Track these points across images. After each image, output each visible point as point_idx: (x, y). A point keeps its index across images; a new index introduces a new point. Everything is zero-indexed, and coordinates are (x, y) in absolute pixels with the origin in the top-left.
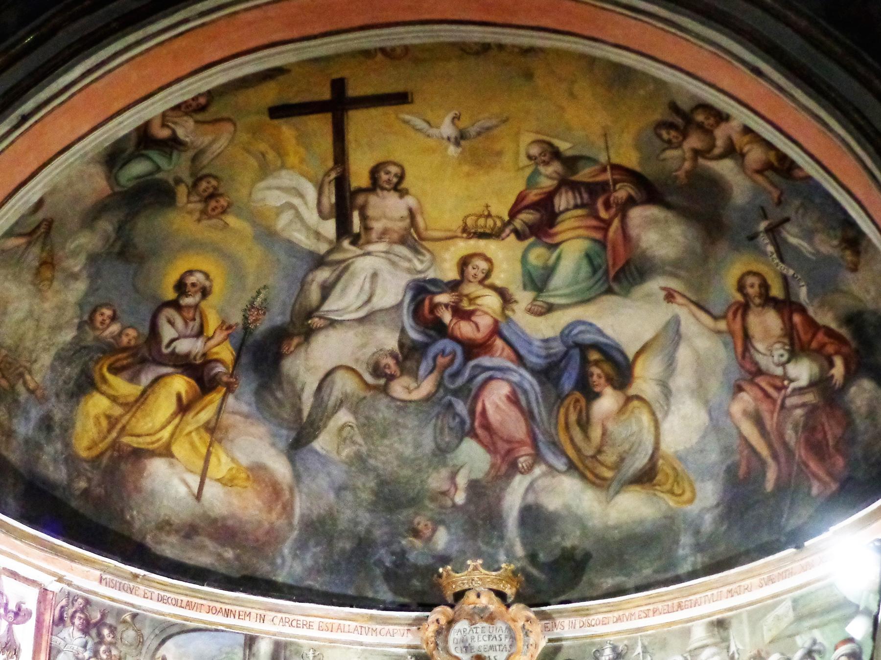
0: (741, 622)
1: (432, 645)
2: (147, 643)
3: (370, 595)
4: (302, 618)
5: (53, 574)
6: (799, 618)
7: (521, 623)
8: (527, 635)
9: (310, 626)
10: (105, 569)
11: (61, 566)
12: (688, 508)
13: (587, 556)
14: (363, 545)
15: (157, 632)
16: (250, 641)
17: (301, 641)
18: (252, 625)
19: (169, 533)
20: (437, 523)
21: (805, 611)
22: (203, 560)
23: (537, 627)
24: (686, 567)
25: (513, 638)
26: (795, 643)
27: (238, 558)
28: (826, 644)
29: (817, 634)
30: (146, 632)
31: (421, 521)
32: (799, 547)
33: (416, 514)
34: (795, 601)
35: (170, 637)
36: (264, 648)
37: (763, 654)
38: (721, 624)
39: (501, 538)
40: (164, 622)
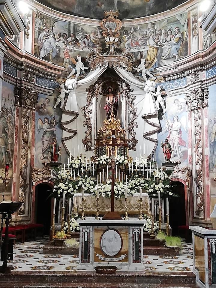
0: (157, 24)
1: (102, 26)
2: (52, 23)
3: (90, 16)
4: (79, 20)
5: (35, 8)
6: (168, 23)
7: (118, 23)
8: (119, 25)
9: (80, 21)
10: (44, 7)
11: (37, 6)
12: (148, 3)
13: (130, 11)
14: (89, 7)
15: (53, 21)
16: (70, 23)
17: (78, 24)
18: (70, 20)
19: (54, 2)
20: (102, 3)
21: (170, 22)
22: (61, 8)
23: (121, 23)
24: (147, 14)
25: (117, 25)
26: (167, 28)
27: (67, 8)
28: (174, 28)
29: (171, 26)
30: (51, 20)
31: (99, 3)
32: (170, 9)
33: (99, 2)
34: (168, 20)
35: (55, 22)
36: (72, 25)
37: (161, 30)
38: (153, 24)
39: (114, 7)
40: (55, 19)
